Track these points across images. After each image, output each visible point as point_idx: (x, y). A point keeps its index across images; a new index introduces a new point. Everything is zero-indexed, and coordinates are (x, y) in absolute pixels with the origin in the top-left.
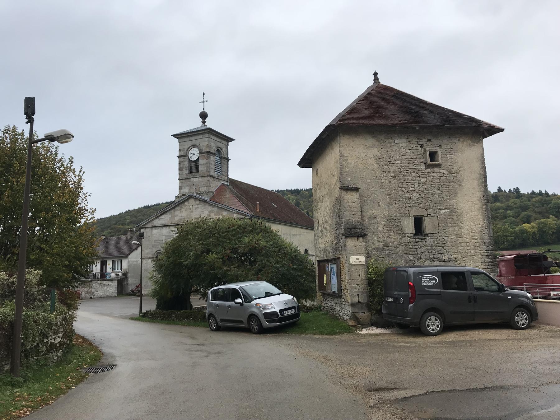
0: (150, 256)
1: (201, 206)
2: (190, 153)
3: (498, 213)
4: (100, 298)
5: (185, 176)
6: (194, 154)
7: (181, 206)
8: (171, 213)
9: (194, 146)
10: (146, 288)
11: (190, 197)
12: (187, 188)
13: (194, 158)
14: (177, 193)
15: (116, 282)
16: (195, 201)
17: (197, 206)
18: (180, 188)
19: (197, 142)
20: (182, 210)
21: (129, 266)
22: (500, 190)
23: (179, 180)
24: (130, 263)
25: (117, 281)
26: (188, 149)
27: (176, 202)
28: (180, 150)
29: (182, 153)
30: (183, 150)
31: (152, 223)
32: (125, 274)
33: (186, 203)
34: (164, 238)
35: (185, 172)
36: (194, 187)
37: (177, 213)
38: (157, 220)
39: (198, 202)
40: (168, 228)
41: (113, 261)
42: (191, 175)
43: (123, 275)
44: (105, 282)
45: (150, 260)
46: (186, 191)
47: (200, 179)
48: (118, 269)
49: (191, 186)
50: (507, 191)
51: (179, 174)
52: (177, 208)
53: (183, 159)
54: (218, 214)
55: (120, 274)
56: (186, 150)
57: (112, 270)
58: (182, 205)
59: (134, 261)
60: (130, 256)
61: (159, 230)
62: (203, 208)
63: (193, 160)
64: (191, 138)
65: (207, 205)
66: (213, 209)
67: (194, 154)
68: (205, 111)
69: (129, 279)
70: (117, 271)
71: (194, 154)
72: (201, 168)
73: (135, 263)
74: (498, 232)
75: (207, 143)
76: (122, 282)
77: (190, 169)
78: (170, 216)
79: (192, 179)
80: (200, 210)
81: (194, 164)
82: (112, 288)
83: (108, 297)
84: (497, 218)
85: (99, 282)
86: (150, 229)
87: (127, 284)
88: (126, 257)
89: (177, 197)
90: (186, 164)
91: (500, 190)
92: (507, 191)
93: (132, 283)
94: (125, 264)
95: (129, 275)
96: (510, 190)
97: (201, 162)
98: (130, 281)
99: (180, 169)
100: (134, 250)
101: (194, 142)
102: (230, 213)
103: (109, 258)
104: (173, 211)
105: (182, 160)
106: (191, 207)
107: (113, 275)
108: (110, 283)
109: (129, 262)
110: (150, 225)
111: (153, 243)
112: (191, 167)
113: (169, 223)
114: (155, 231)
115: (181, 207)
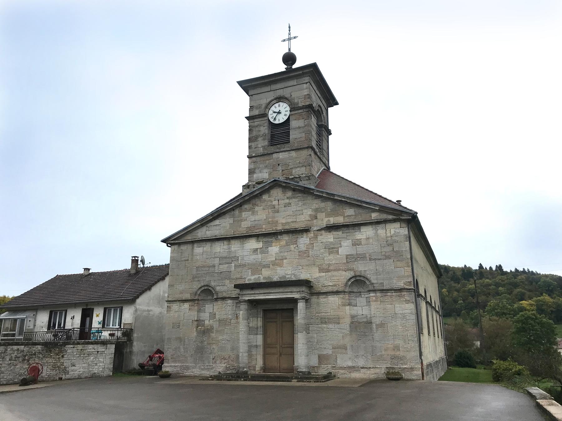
0: (187, 296)
1: (296, 200)
2: (271, 112)
3: (490, 289)
4: (79, 378)
5: (261, 151)
6: (279, 113)
7: (253, 201)
8: (233, 216)
9: (280, 99)
10: (175, 361)
11: (276, 184)
12: (265, 171)
13: (281, 119)
14: (245, 181)
15: (112, 348)
16: (284, 192)
17: (287, 201)
18: (251, 172)
19: (286, 93)
20: (257, 208)
21: (136, 319)
22: (481, 266)
23: (249, 157)
24: (139, 312)
25: (114, 346)
26: (269, 105)
27: (244, 194)
28: (251, 108)
29: (256, 112)
30: (259, 107)
31: (194, 234)
32: (128, 333)
33: (265, 197)
34: (217, 261)
35: (262, 143)
36: (280, 168)
37: (244, 214)
38: (204, 229)
39: (289, 194)
40: (226, 242)
41: (105, 310)
42: (272, 149)
43: (124, 334)
44: (91, 346)
45: (186, 305)
46: (264, 175)
47: (293, 154)
48: (113, 324)
49: (274, 168)
50: (488, 269)
51: (250, 147)
52: (246, 206)
53: (257, 122)
54: (333, 213)
55: (119, 334)
56: (263, 106)
57: (103, 327)
58: (257, 201)
59: (144, 311)
60: (138, 301)
61: (207, 247)
62: (300, 203)
63: (277, 122)
64: (274, 87)
65: (310, 198)
66: (323, 205)
67: (279, 113)
68: (292, 51)
69: (135, 343)
70: (111, 326)
71: (280, 113)
72: (294, 135)
73: (145, 314)
74: (497, 309)
75: (306, 92)
76: (122, 346)
77: (268, 138)
78: (231, 221)
79: (275, 156)
80: (293, 208)
81: (280, 130)
82: (102, 361)
83: (94, 379)
84: (489, 294)
85: (80, 347)
86: (189, 247)
87: (131, 352)
88: (132, 301)
89: (245, 187)
90: (264, 130)
91: (481, 266)
92: (488, 269)
93: (139, 354)
94: (128, 315)
95: (135, 335)
96: (491, 268)
97: (294, 124)
98: (137, 346)
99: (251, 140)
100: (158, 281)
101: (280, 93)
102: (361, 211)
103: (98, 304)
104: (237, 212)
105: (256, 124)
106: (275, 203)
107: (105, 334)
108: (100, 348)
109: (136, 310)
110: (189, 238)
111: (194, 272)
112: (273, 137)
113: (230, 234)
114: (198, 250)
115: (255, 205)
